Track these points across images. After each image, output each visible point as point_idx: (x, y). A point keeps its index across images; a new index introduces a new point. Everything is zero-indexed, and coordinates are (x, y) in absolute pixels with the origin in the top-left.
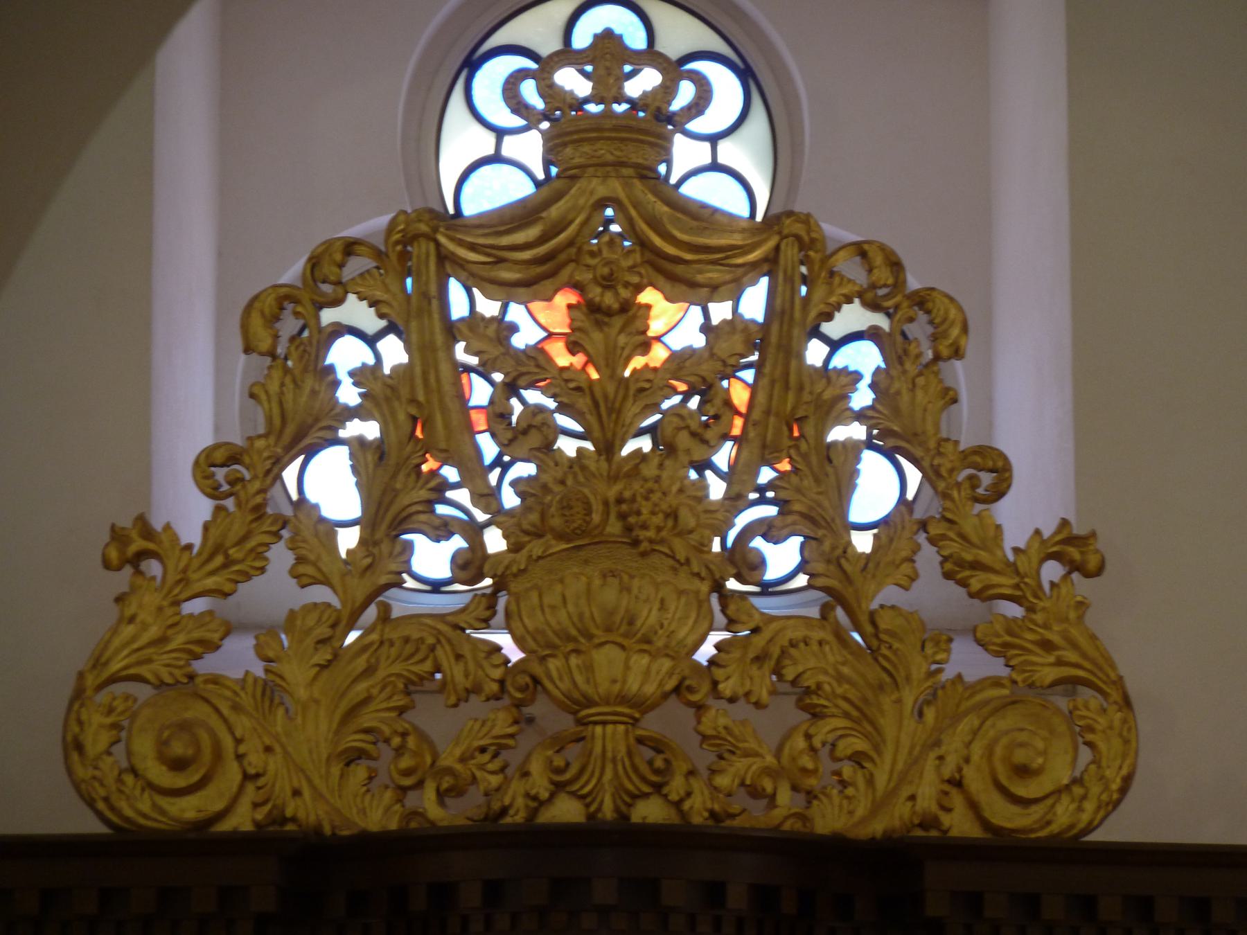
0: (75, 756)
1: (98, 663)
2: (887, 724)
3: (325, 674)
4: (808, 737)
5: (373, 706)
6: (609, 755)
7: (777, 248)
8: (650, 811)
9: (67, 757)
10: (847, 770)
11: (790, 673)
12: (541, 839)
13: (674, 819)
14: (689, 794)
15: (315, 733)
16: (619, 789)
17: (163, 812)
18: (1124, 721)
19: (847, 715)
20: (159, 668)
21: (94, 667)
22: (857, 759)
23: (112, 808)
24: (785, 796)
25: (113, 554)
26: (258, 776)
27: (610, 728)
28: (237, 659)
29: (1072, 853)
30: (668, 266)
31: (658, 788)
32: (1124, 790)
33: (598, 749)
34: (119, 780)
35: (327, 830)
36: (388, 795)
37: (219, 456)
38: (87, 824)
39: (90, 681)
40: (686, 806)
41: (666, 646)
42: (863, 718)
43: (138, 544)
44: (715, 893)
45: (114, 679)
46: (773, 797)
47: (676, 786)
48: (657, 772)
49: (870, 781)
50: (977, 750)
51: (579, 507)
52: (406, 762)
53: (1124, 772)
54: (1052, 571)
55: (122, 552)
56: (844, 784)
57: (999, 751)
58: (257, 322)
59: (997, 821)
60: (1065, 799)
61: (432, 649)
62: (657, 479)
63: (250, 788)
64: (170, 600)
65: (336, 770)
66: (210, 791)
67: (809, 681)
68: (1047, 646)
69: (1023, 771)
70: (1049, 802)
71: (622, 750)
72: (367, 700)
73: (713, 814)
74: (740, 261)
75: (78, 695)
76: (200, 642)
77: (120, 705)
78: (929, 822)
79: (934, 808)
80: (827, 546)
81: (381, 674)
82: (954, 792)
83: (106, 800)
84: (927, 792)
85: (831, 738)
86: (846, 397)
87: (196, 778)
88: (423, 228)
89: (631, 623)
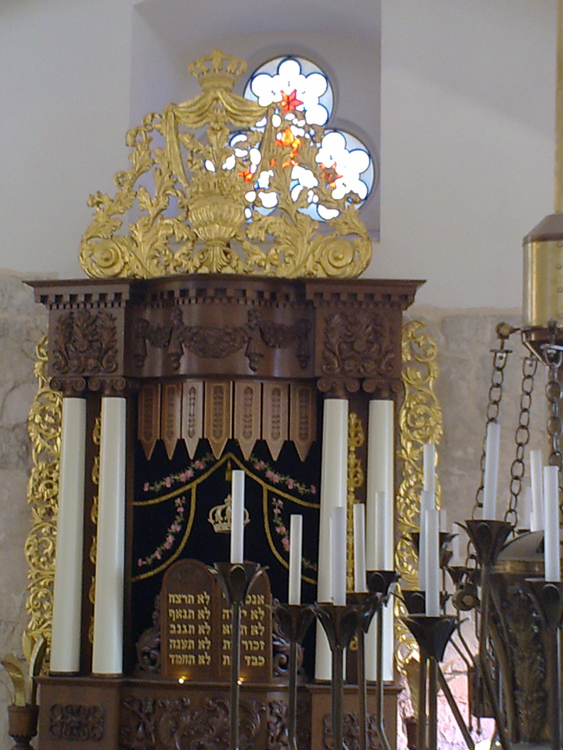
1: (87, 233)
2: (299, 246)
4: (276, 250)
8: (228, 270)
10: (287, 260)
13: (233, 272)
19: (287, 244)
22: (290, 255)
23: (90, 273)
24: (268, 267)
25: (90, 203)
32: (367, 265)
35: (145, 278)
39: (85, 237)
42: (293, 244)
45: (91, 237)
46: (265, 267)
47: (234, 263)
51: (206, 185)
52: (165, 259)
55: (92, 202)
57: (330, 253)
59: (330, 273)
66: (115, 267)
67: (276, 234)
68: (346, 223)
73: (245, 271)
75: (82, 242)
77: (93, 243)
79: (312, 270)
80: (282, 196)
82: (319, 265)
84: (310, 265)
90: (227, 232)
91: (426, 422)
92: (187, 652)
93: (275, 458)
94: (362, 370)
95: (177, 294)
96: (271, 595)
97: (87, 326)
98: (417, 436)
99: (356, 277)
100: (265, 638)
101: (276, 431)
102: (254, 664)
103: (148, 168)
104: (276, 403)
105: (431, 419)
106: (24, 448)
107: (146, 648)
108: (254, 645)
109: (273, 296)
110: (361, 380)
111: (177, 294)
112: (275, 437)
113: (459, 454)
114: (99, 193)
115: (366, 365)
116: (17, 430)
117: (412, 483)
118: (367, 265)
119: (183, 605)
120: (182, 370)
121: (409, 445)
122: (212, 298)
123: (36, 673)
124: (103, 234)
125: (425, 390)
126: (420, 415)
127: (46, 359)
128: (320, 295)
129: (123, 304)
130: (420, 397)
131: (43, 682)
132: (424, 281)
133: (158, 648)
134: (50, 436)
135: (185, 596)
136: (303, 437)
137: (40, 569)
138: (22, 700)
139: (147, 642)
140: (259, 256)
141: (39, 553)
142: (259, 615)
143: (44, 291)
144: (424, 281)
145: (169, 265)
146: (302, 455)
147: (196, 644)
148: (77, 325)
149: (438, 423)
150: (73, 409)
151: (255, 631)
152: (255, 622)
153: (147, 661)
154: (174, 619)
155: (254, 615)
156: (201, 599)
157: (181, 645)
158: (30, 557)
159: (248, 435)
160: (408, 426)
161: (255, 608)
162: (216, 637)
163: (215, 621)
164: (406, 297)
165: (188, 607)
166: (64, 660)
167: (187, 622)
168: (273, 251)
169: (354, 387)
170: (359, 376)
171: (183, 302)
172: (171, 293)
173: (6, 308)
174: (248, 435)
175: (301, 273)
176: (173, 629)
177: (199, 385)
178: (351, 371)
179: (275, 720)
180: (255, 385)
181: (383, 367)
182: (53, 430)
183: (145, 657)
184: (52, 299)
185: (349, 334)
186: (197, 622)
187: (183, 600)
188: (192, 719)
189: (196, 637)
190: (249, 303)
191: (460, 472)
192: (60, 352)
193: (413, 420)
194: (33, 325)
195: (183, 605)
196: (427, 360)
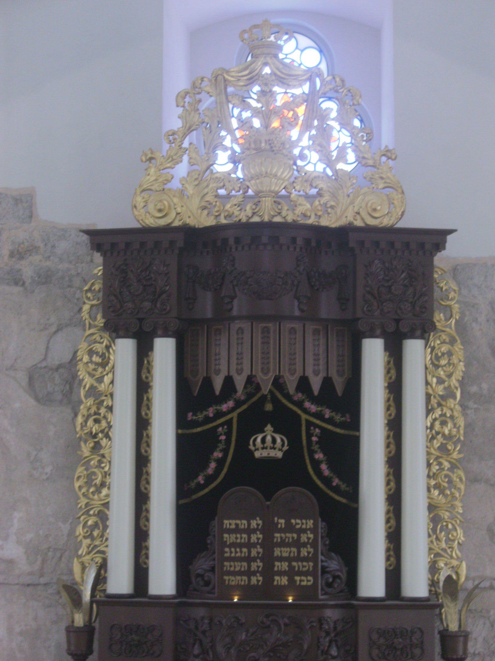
0: (135, 209)
4: (319, 201)
5: (208, 195)
8: (278, 219)
9: (133, 209)
10: (329, 210)
12: (248, 226)
15: (195, 203)
17: (156, 223)
18: (402, 197)
22: (332, 207)
26: (179, 213)
27: (267, 198)
28: (175, 184)
31: (279, 213)
32: (402, 215)
34: (145, 215)
36: (213, 217)
37: (170, 133)
40: (287, 217)
43: (150, 155)
44: (294, 240)
46: (310, 217)
48: (279, 209)
49: (336, 213)
50: (364, 205)
53: (402, 210)
54: (384, 159)
56: (329, 214)
57: (369, 205)
58: (180, 99)
59: (368, 223)
60: (386, 217)
63: (178, 216)
65: (199, 211)
66: (168, 217)
68: (382, 178)
69: (375, 210)
72: (207, 193)
74: (301, 79)
76: (166, 180)
78: (350, 224)
79: (352, 219)
81: (210, 186)
83: (142, 220)
85: (325, 201)
86: (329, 114)
87: (164, 214)
88: (219, 72)
91: (449, 360)
92: (240, 573)
93: (316, 393)
94: (399, 311)
95: (231, 241)
96: (320, 520)
98: (442, 373)
100: (314, 559)
101: (316, 368)
102: (304, 583)
103: (198, 127)
104: (317, 343)
105: (454, 357)
106: (68, 387)
107: (199, 571)
108: (303, 566)
110: (397, 321)
111: (231, 241)
112: (316, 373)
113: (474, 389)
114: (150, 149)
115: (402, 307)
116: (61, 370)
117: (437, 416)
118: (402, 215)
119: (237, 530)
120: (235, 312)
121: (435, 380)
123: (93, 595)
125: (448, 330)
126: (443, 354)
127: (95, 302)
128: (362, 243)
129: (177, 252)
130: (444, 337)
131: (99, 603)
132: (455, 231)
133: (213, 569)
134: (98, 374)
135: (238, 522)
136: (340, 373)
137: (89, 498)
138: (79, 620)
139: (201, 564)
140: (305, 206)
141: (89, 483)
142: (308, 538)
144: (455, 231)
145: (219, 215)
146: (339, 390)
147: (249, 566)
148: (132, 271)
149: (460, 361)
150: (125, 349)
151: (304, 552)
152: (304, 545)
153: (201, 583)
154: (228, 543)
155: (304, 538)
156: (254, 524)
157: (235, 567)
158: (80, 488)
159: (292, 372)
160: (432, 363)
161: (305, 531)
162: (268, 559)
163: (268, 544)
165: (244, 531)
166: (120, 583)
167: (241, 546)
168: (317, 203)
169: (391, 328)
170: (397, 317)
171: (236, 250)
172: (225, 241)
173: (49, 257)
174: (292, 372)
176: (227, 552)
177: (246, 325)
178: (389, 312)
179: (323, 634)
180: (297, 325)
181: (418, 309)
182: (100, 370)
183: (199, 579)
185: (387, 278)
186: (249, 545)
187: (237, 525)
188: (246, 635)
189: (249, 559)
190: (298, 250)
191: (475, 406)
192: (115, 296)
193: (438, 358)
194: (73, 272)
195: (237, 530)
196: (448, 303)
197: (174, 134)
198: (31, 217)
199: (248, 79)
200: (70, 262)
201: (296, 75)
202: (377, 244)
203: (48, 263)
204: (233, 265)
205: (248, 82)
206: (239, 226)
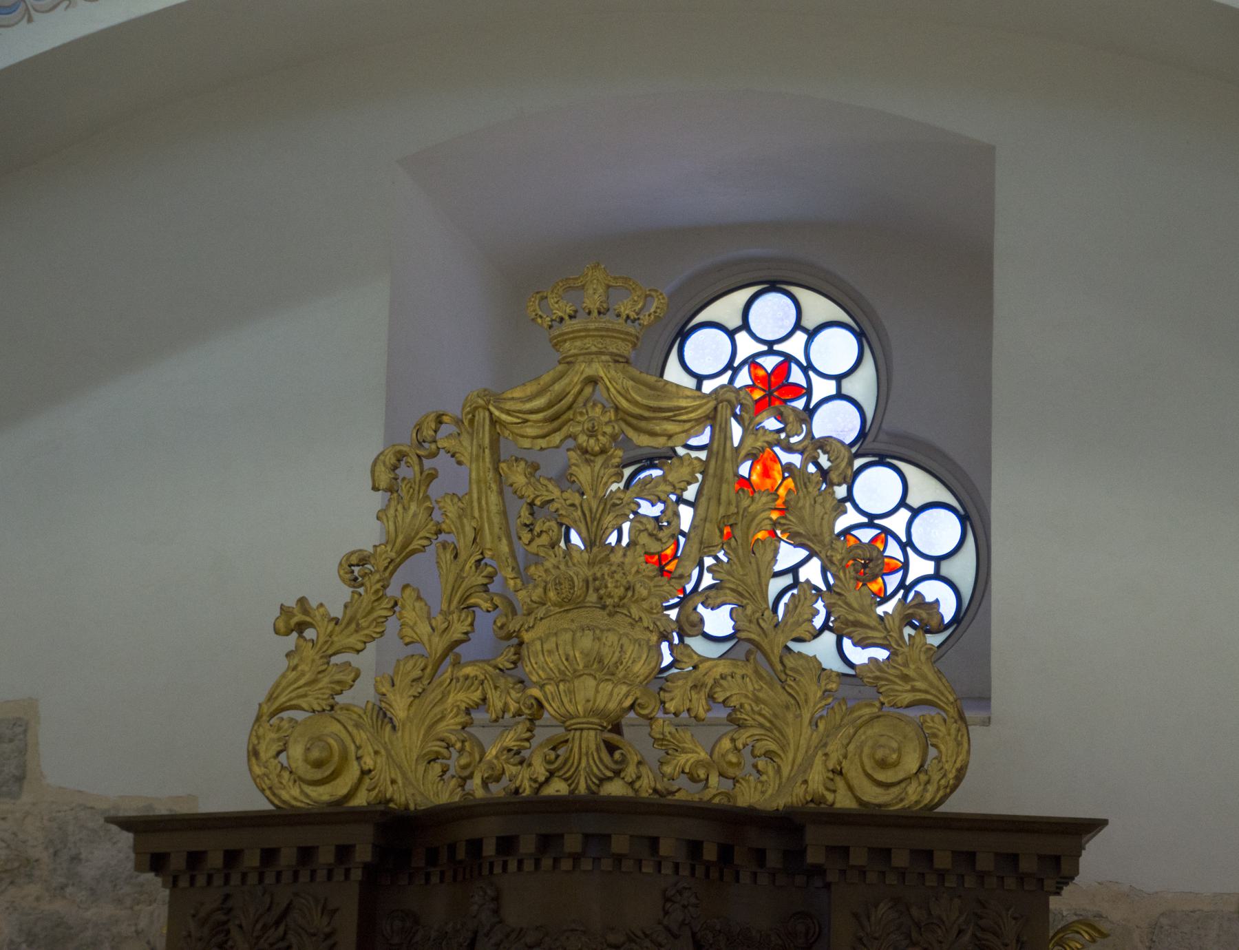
0: (254, 760)
1: (271, 698)
2: (789, 732)
3: (417, 701)
4: (733, 740)
6: (584, 750)
7: (715, 409)
8: (615, 789)
9: (249, 760)
10: (761, 764)
11: (720, 697)
13: (631, 793)
14: (639, 778)
15: (410, 742)
16: (590, 773)
17: (307, 796)
19: (761, 726)
20: (312, 701)
21: (269, 700)
22: (769, 755)
23: (274, 794)
24: (714, 780)
25: (281, 625)
26: (370, 771)
29: (927, 821)
30: (643, 424)
31: (617, 773)
32: (959, 778)
33: (576, 749)
35: (412, 807)
37: (354, 560)
38: (261, 804)
40: (637, 785)
41: (625, 677)
42: (772, 727)
43: (299, 617)
47: (630, 772)
48: (616, 762)
49: (778, 771)
51: (566, 585)
52: (463, 761)
53: (958, 765)
55: (287, 623)
57: (866, 750)
58: (380, 468)
59: (866, 798)
60: (914, 784)
61: (482, 683)
62: (621, 565)
64: (320, 654)
66: (339, 781)
67: (734, 702)
69: (883, 764)
70: (903, 785)
71: (593, 747)
73: (655, 791)
74: (684, 417)
75: (258, 719)
77: (285, 725)
78: (818, 800)
79: (821, 790)
80: (749, 610)
82: (838, 778)
83: (270, 788)
84: (817, 777)
87: (328, 773)
88: (481, 402)
89: (601, 661)
90: (612, 697)
97: (265, 928)
99: (932, 807)
103: (425, 542)
109: (726, 853)
111: (489, 849)
114: (302, 601)
122: (576, 858)
124: (314, 700)
129: (357, 874)
143: (160, 843)
144: (1104, 823)
145: (471, 776)
148: (240, 926)
164: (1057, 860)
171: (505, 868)
172: (475, 846)
173: (63, 887)
175: (794, 796)
184: (177, 862)
190: (667, 870)
197: (363, 561)
198: (20, 779)
199: (546, 420)
200: (119, 901)
201: (669, 410)
202: (884, 854)
203: (59, 906)
204: (496, 912)
205: (549, 427)
206: (521, 807)
